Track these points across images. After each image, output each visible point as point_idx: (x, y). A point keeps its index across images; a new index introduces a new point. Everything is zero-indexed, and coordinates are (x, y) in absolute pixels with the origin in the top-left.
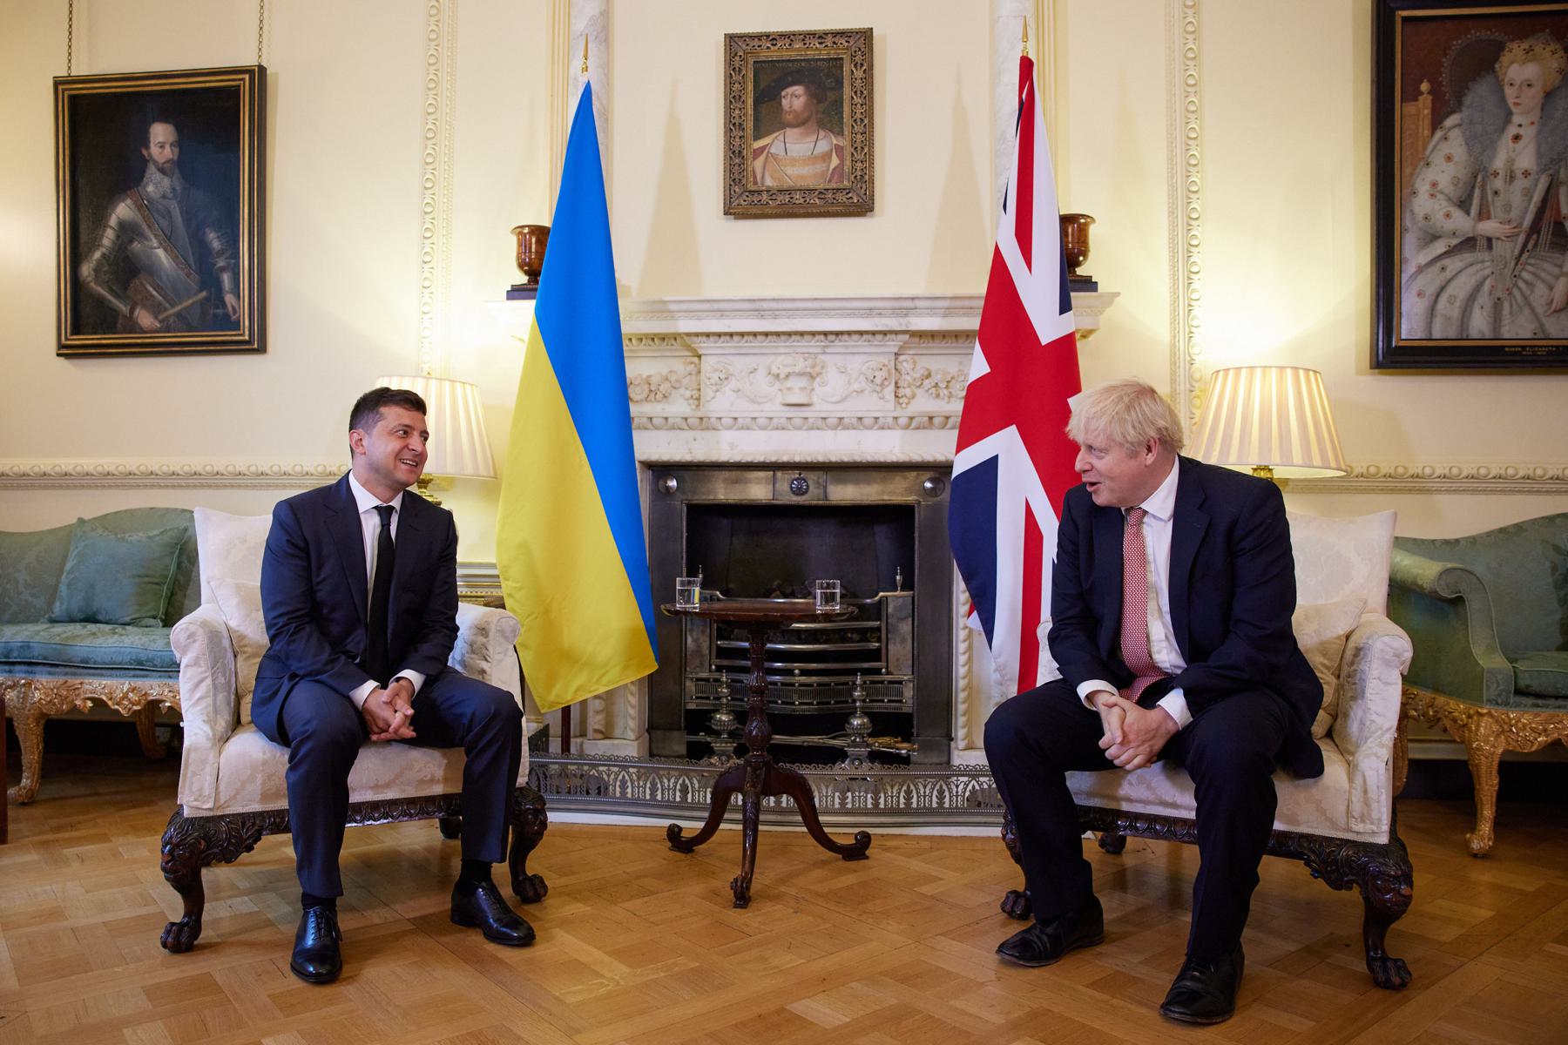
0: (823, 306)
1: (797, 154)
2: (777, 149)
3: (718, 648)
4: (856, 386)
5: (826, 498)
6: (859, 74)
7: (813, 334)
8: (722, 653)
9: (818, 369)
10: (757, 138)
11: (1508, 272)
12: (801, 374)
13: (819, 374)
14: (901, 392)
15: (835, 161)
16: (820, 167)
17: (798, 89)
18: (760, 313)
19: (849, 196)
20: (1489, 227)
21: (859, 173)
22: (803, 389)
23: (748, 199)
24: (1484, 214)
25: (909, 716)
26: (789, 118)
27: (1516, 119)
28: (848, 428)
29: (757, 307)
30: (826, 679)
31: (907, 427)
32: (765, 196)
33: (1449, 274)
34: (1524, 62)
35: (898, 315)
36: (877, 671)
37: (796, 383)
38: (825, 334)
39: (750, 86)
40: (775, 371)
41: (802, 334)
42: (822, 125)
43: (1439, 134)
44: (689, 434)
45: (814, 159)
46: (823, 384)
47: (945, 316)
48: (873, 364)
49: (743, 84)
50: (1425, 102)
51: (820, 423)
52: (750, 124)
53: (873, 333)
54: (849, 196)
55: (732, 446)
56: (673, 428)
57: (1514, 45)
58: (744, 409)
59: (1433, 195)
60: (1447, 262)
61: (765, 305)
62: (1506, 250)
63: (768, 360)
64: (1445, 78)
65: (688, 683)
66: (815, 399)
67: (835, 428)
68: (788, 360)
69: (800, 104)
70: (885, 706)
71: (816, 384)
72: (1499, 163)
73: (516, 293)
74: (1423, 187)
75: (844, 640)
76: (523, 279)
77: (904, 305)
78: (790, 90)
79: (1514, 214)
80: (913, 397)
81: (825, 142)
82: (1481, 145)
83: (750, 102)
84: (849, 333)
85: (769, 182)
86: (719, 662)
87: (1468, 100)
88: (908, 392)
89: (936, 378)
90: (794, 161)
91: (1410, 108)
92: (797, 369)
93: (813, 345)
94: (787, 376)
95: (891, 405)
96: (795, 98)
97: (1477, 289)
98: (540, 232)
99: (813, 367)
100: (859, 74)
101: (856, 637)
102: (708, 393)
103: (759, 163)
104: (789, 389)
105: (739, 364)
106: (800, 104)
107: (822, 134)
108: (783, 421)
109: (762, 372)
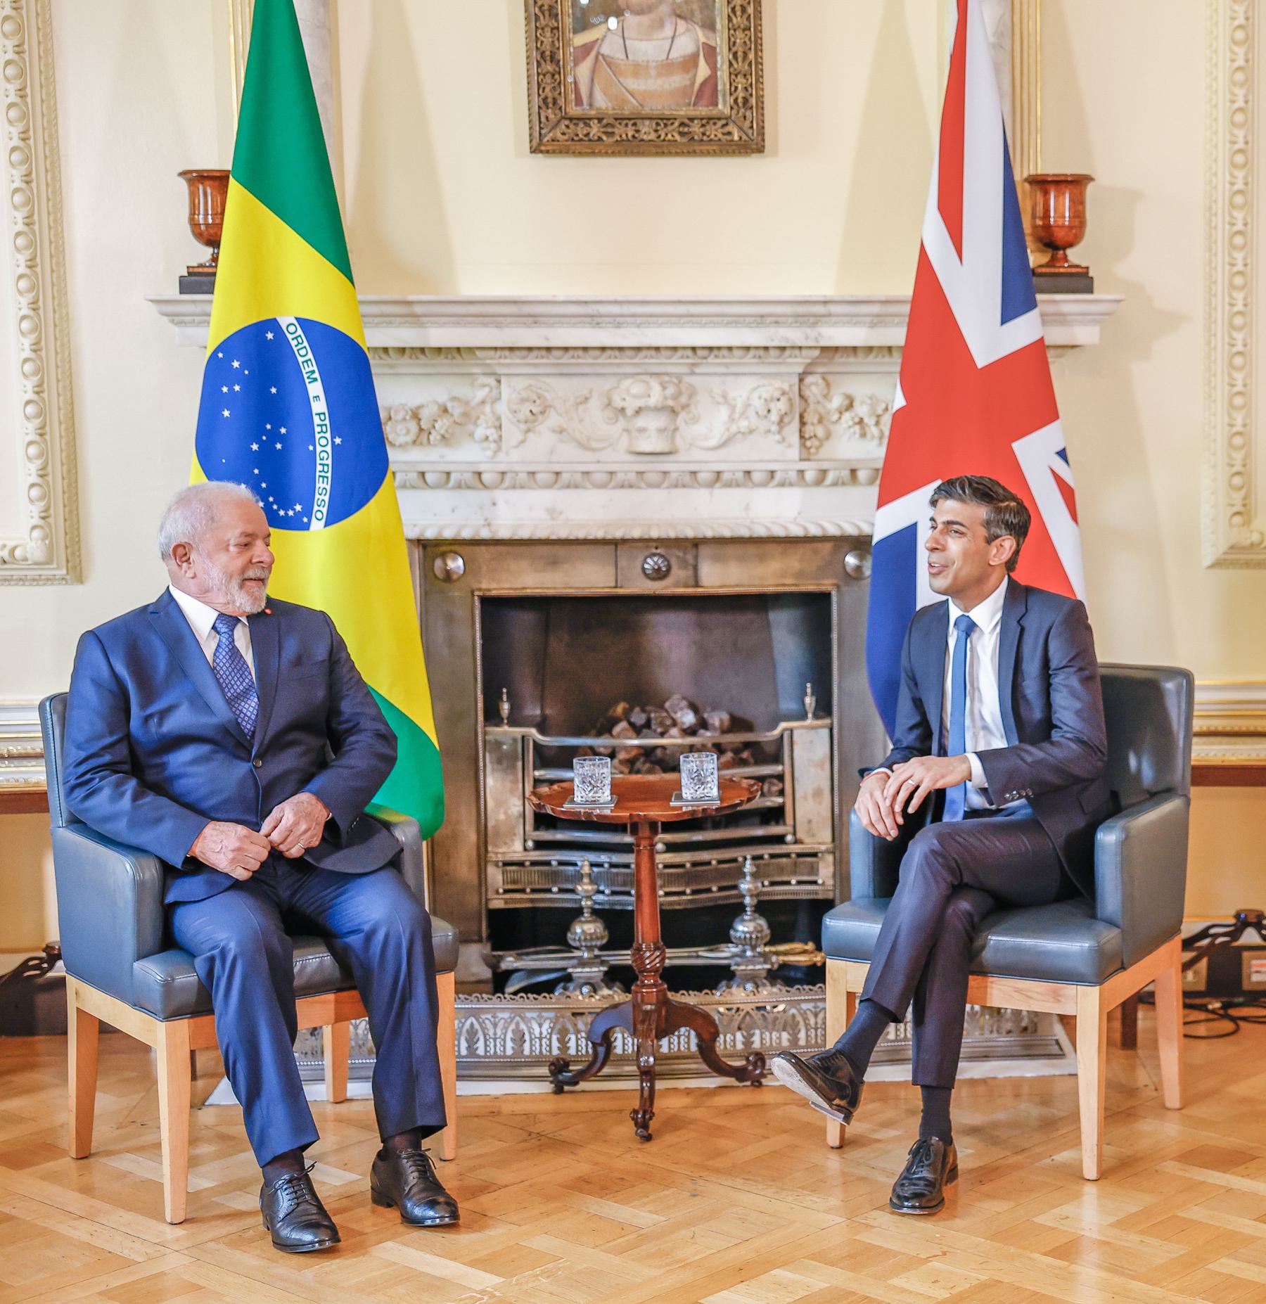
4: (744, 424)
5: (697, 585)
9: (683, 399)
12: (658, 409)
13: (685, 407)
14: (809, 430)
19: (724, 120)
21: (741, 94)
22: (661, 431)
23: (566, 123)
28: (729, 485)
30: (704, 856)
35: (802, 324)
36: (780, 839)
37: (652, 423)
40: (618, 403)
44: (484, 496)
46: (695, 420)
48: (766, 392)
51: (687, 478)
55: (553, 513)
56: (459, 486)
58: (570, 457)
63: (607, 384)
65: (491, 870)
66: (679, 442)
68: (636, 388)
71: (680, 421)
80: (828, 436)
81: (687, 40)
85: (601, 102)
88: (820, 432)
89: (861, 410)
90: (639, 70)
92: (652, 402)
93: (676, 365)
94: (638, 411)
95: (794, 453)
99: (676, 397)
102: (512, 433)
104: (642, 430)
105: (560, 389)
108: (632, 477)
109: (595, 405)
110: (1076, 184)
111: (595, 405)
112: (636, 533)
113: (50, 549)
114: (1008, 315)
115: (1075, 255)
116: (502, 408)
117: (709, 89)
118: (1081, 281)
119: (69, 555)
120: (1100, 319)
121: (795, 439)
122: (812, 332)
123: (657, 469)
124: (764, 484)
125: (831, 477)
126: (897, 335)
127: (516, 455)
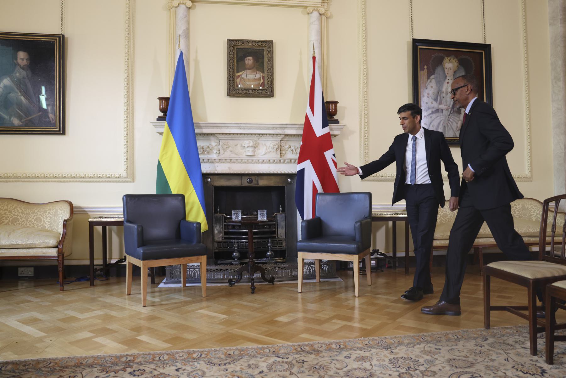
0: (259, 126)
1: (250, 78)
2: (244, 76)
3: (225, 232)
4: (269, 150)
6: (269, 54)
7: (255, 134)
8: (226, 233)
10: (238, 72)
11: (447, 119)
12: (252, 146)
15: (262, 81)
16: (257, 83)
17: (250, 58)
18: (240, 128)
19: (266, 91)
20: (442, 107)
23: (234, 91)
24: (441, 103)
25: (285, 251)
26: (247, 67)
27: (448, 78)
28: (265, 163)
29: (239, 126)
31: (284, 163)
32: (240, 91)
33: (433, 119)
34: (449, 63)
37: (251, 149)
38: (259, 134)
39: (235, 56)
40: (243, 145)
41: (252, 134)
42: (258, 69)
43: (429, 80)
45: (255, 80)
47: (297, 130)
48: (273, 144)
49: (233, 55)
50: (426, 71)
52: (235, 68)
53: (274, 134)
54: (266, 91)
55: (229, 168)
56: (211, 163)
57: (446, 58)
58: (234, 157)
59: (428, 97)
60: (431, 115)
61: (242, 125)
62: (446, 113)
63: (241, 142)
64: (430, 65)
67: (262, 163)
68: (247, 142)
69: (250, 62)
70: (277, 248)
72: (444, 90)
73: (160, 119)
74: (426, 95)
75: (264, 228)
76: (162, 114)
77: (283, 126)
78: (248, 58)
79: (448, 103)
81: (259, 75)
82: (440, 84)
83: (235, 61)
84: (266, 134)
86: (226, 236)
87: (436, 72)
88: (284, 152)
89: (292, 148)
90: (249, 80)
91: (422, 73)
92: (251, 145)
93: (255, 138)
94: (248, 147)
95: (279, 156)
96: (249, 61)
97: (439, 123)
98: (166, 99)
100: (269, 54)
101: (268, 227)
102: (222, 151)
103: (238, 80)
105: (231, 143)
106: (250, 62)
107: (258, 72)
110: (335, 103)
111: (238, 146)
112: (247, 172)
113: (128, 175)
114: (323, 128)
115: (335, 117)
116: (220, 147)
117: (263, 85)
118: (337, 122)
119: (130, 176)
120: (340, 129)
121: (279, 154)
122: (283, 131)
123: (251, 159)
124: (273, 163)
125: (286, 161)
126: (301, 132)
127: (223, 156)
